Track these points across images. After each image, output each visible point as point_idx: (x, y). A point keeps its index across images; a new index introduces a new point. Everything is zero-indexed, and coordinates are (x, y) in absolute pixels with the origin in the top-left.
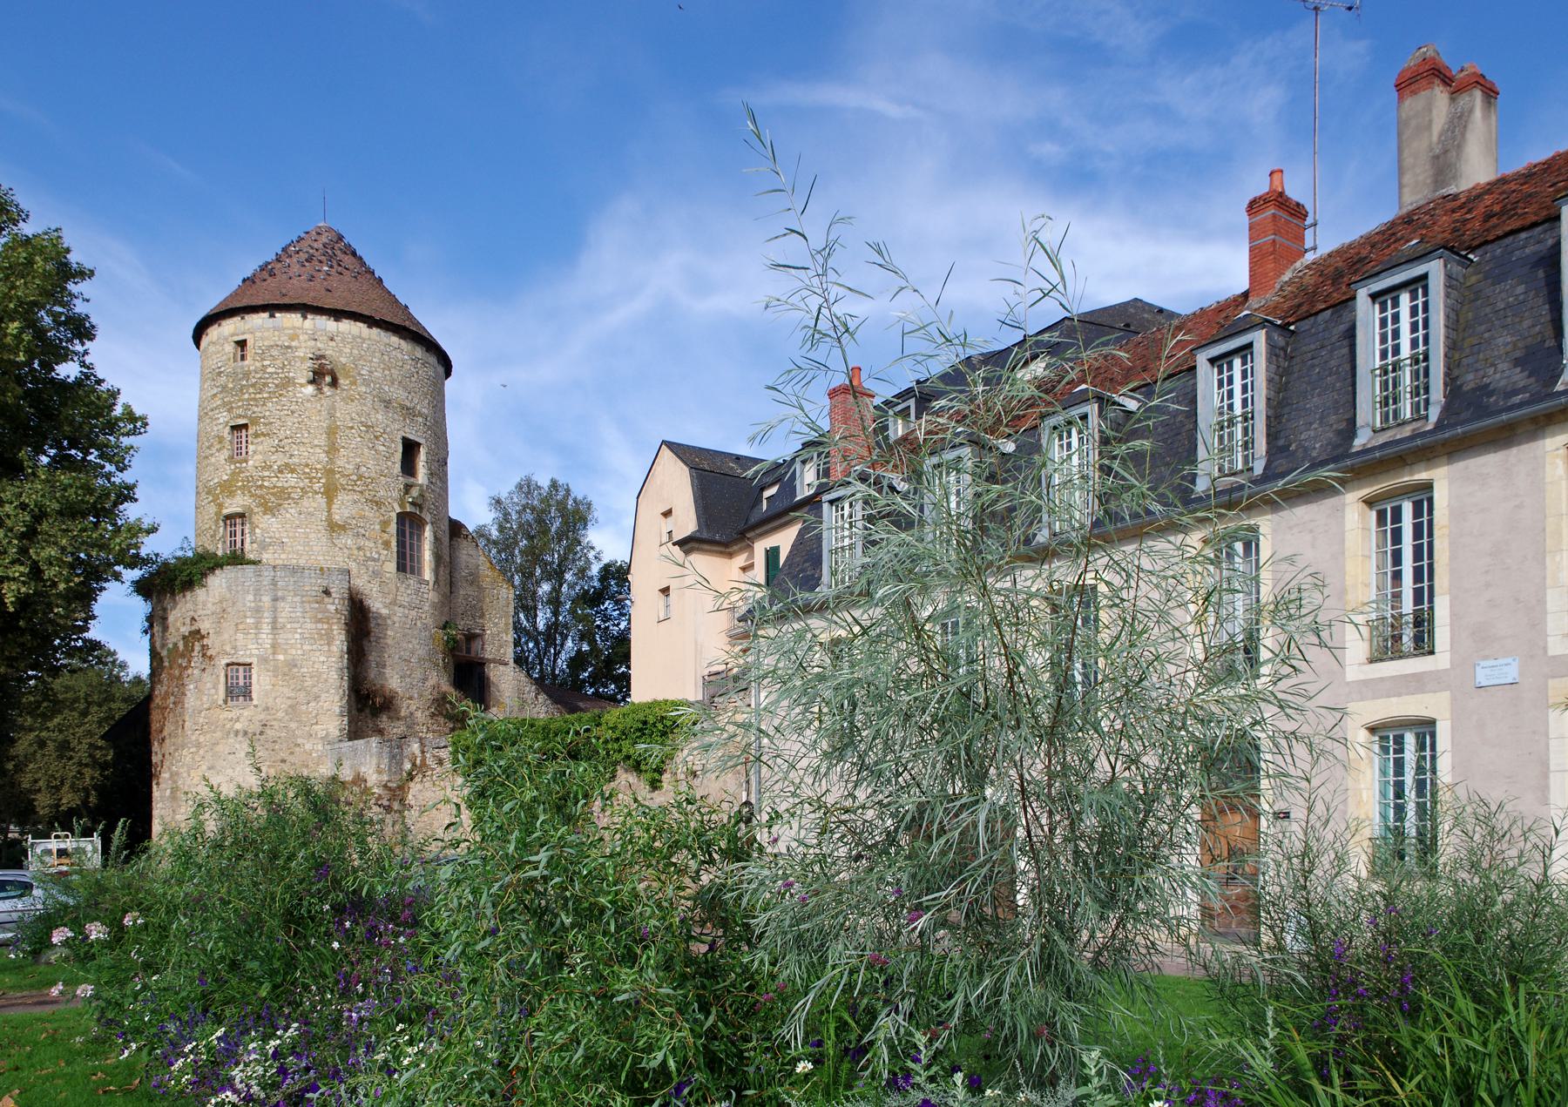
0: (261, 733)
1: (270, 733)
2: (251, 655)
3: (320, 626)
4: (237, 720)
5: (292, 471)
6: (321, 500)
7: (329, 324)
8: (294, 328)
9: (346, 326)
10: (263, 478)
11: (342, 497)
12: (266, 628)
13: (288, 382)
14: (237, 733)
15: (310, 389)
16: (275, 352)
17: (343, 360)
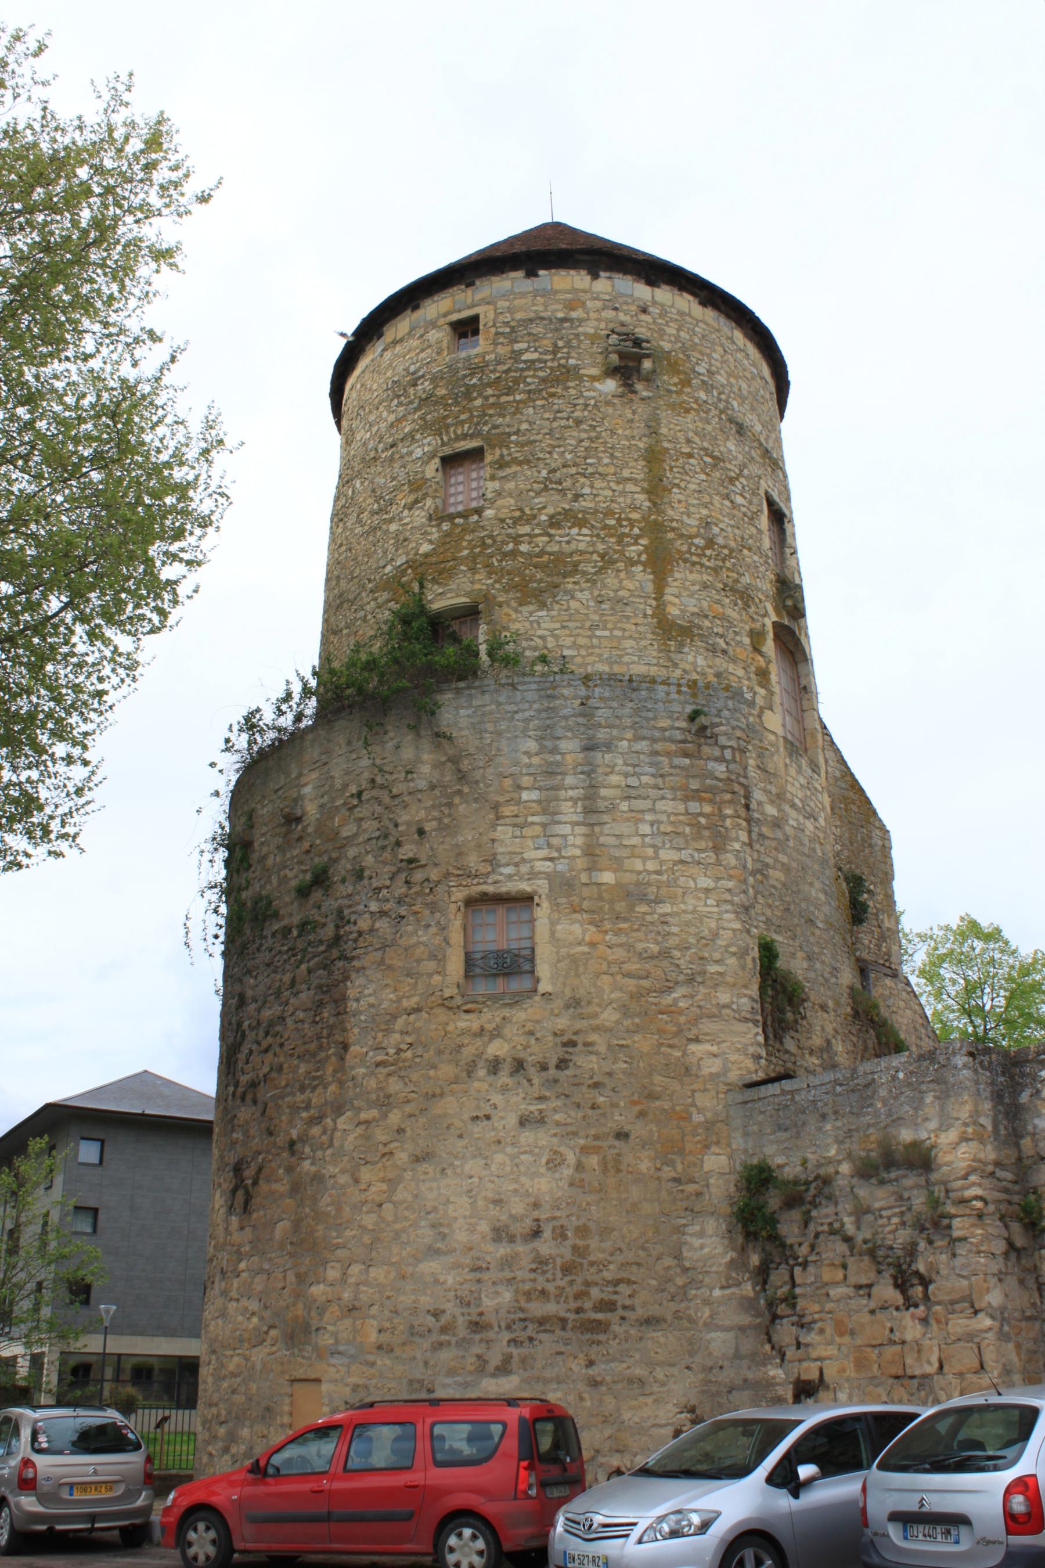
0: (562, 1064)
1: (587, 1063)
2: (533, 875)
3: (694, 807)
4: (496, 1033)
5: (581, 523)
6: (643, 578)
7: (642, 291)
8: (574, 291)
9: (664, 294)
10: (517, 539)
11: (681, 577)
12: (569, 812)
13: (567, 374)
14: (495, 1066)
15: (610, 385)
16: (537, 329)
17: (667, 346)
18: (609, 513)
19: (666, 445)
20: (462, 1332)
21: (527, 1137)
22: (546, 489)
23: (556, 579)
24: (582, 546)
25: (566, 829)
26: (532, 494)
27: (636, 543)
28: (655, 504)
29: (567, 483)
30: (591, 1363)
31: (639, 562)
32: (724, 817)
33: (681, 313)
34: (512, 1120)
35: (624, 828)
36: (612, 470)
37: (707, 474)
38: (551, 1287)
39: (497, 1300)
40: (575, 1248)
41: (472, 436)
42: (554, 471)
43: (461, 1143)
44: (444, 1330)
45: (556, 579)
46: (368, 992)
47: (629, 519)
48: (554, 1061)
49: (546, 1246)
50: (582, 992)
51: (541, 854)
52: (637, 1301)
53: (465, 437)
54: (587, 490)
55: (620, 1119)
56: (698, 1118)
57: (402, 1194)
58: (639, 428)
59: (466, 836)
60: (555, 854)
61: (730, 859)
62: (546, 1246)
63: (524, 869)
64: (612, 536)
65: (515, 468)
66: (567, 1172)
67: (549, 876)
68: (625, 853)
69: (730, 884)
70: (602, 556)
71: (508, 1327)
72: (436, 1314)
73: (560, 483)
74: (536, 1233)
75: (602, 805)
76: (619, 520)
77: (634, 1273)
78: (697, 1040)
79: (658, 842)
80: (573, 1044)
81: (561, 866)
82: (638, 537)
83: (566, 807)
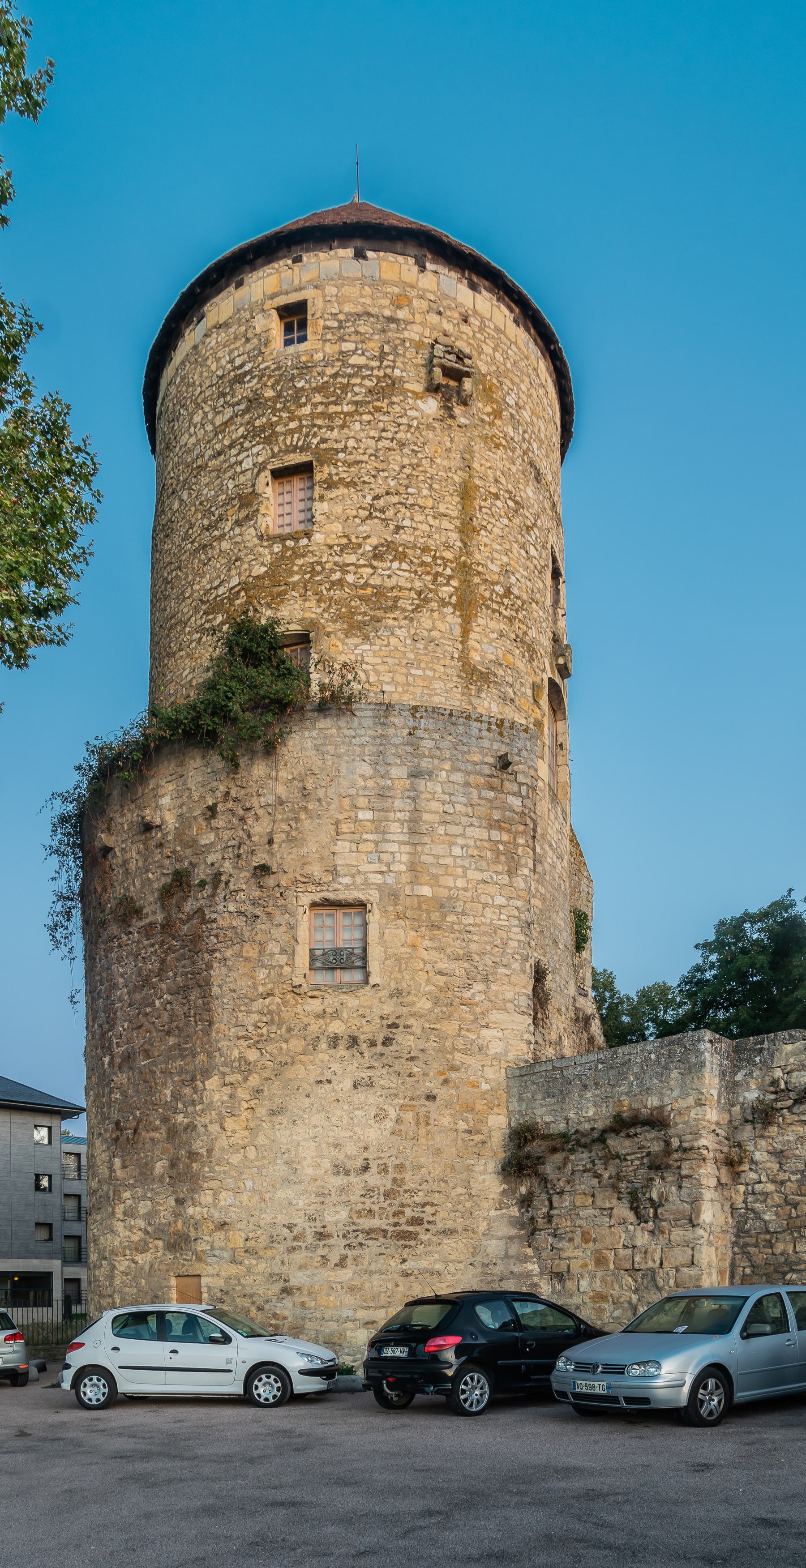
0: (387, 1042)
1: (405, 1041)
3: (495, 835)
5: (401, 557)
6: (452, 619)
18: (425, 549)
19: (477, 482)
20: (310, 1239)
21: (360, 1096)
22: (370, 516)
23: (379, 613)
24: (402, 583)
25: (394, 847)
26: (358, 521)
27: (448, 584)
28: (465, 544)
29: (390, 514)
30: (404, 1261)
31: (450, 603)
32: (516, 846)
33: (497, 330)
34: (348, 1084)
35: (440, 849)
36: (430, 503)
37: (510, 520)
38: (375, 1208)
39: (336, 1217)
40: (394, 1180)
41: (302, 449)
42: (377, 498)
43: (307, 1101)
44: (296, 1238)
45: (379, 613)
46: (230, 979)
47: (443, 558)
48: (380, 1039)
49: (373, 1178)
50: (404, 985)
51: (375, 867)
52: (437, 1219)
53: (294, 449)
54: (407, 523)
55: (431, 1085)
56: (485, 1087)
57: (261, 1140)
58: (456, 461)
59: (311, 847)
60: (385, 869)
61: (520, 883)
62: (373, 1178)
63: (359, 880)
64: (428, 573)
65: (342, 490)
66: (389, 1124)
67: (379, 887)
68: (440, 871)
69: (519, 903)
70: (419, 593)
71: (344, 1236)
72: (290, 1227)
73: (384, 513)
74: (366, 1168)
75: (424, 828)
76: (434, 558)
77: (436, 1198)
78: (487, 1027)
79: (466, 863)
80: (395, 1026)
81: (390, 879)
82: (450, 577)
83: (395, 827)
